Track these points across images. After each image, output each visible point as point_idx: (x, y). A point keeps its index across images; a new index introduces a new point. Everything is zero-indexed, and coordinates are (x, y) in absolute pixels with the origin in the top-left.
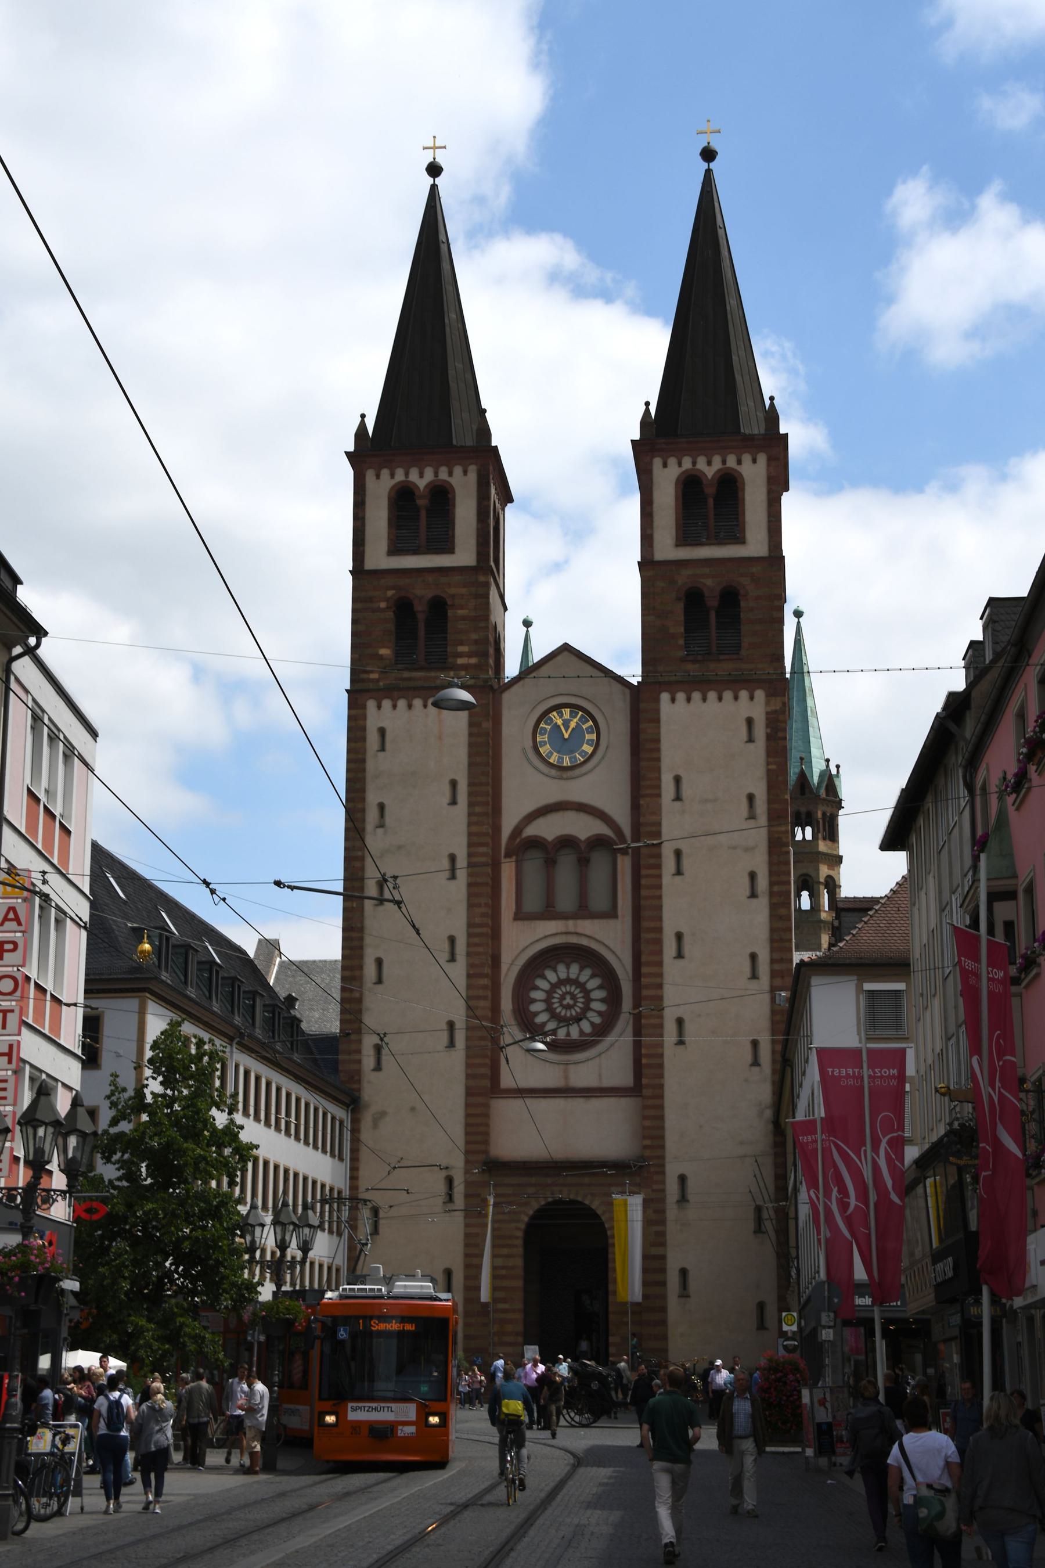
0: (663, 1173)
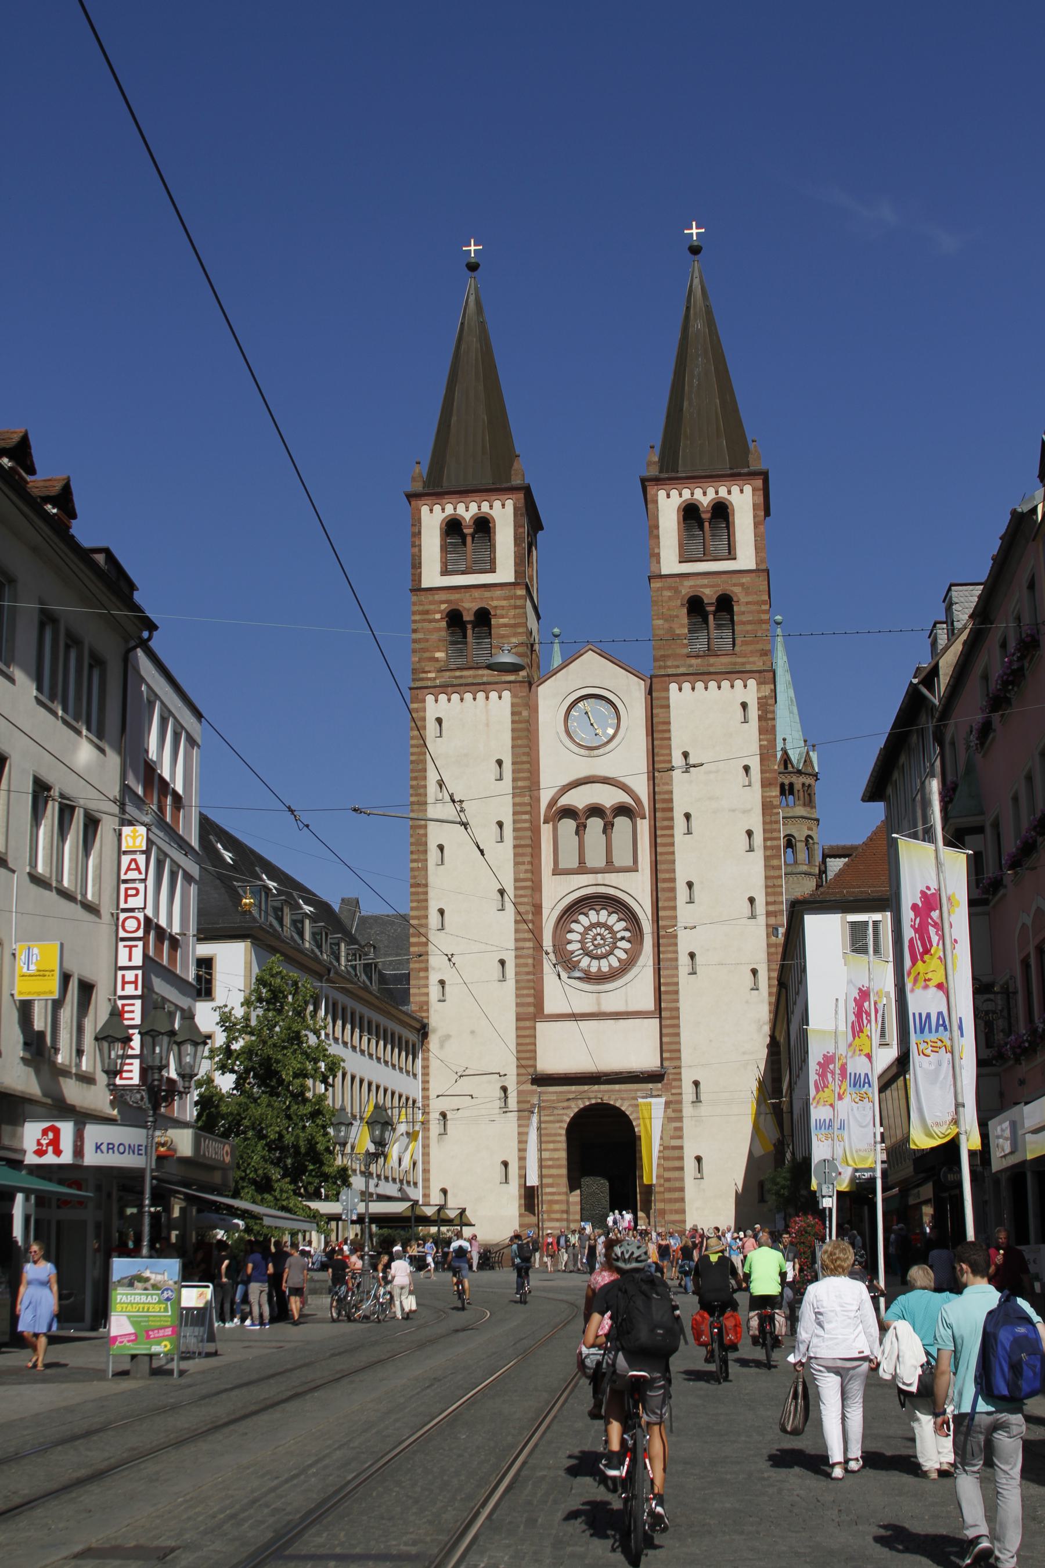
0: (680, 1080)
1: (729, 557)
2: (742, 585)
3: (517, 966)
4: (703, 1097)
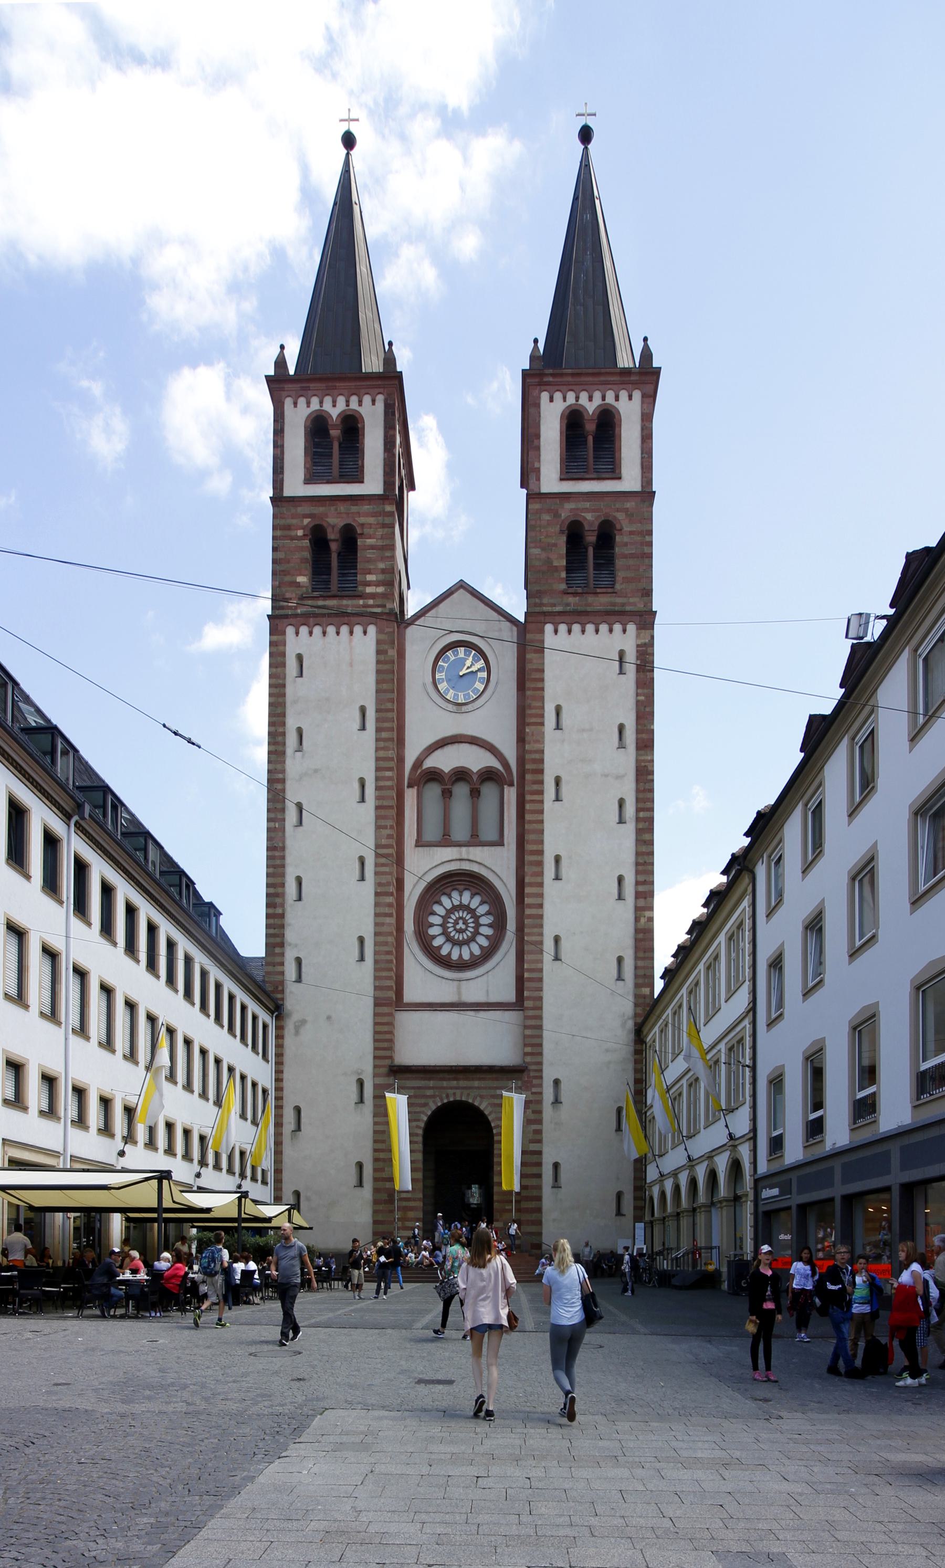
0: (541, 1077)
1: (614, 476)
2: (626, 511)
3: (376, 944)
4: (563, 1098)
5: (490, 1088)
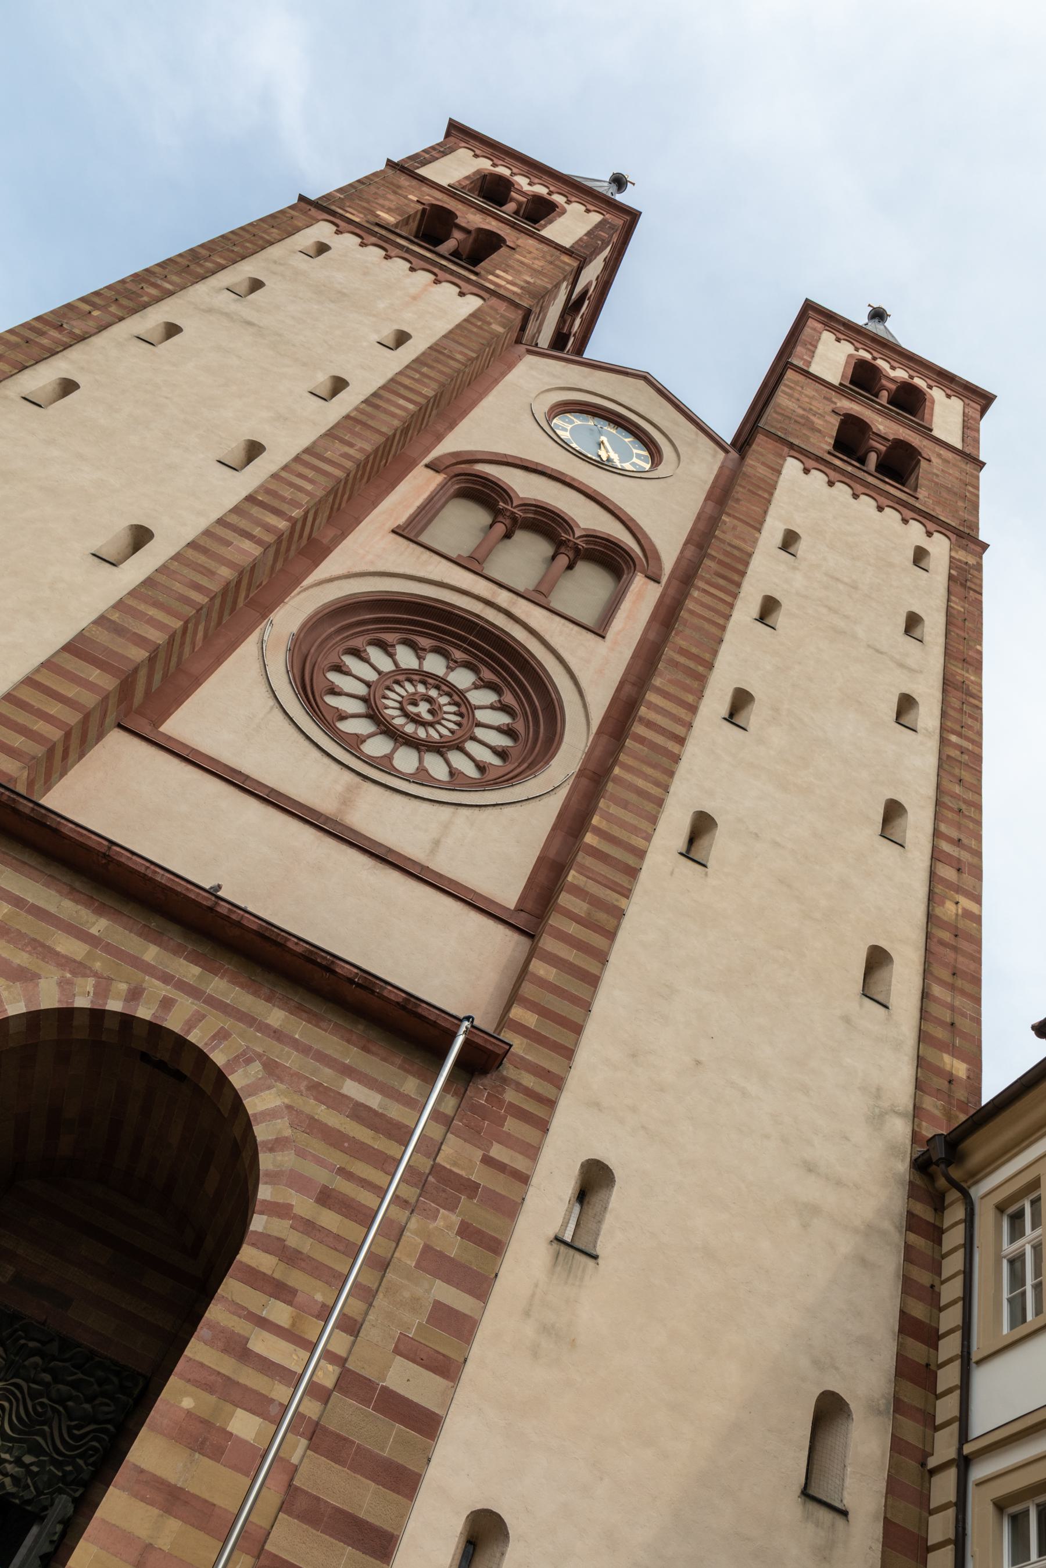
0: (543, 1126)
2: (939, 456)
5: (322, 1058)
